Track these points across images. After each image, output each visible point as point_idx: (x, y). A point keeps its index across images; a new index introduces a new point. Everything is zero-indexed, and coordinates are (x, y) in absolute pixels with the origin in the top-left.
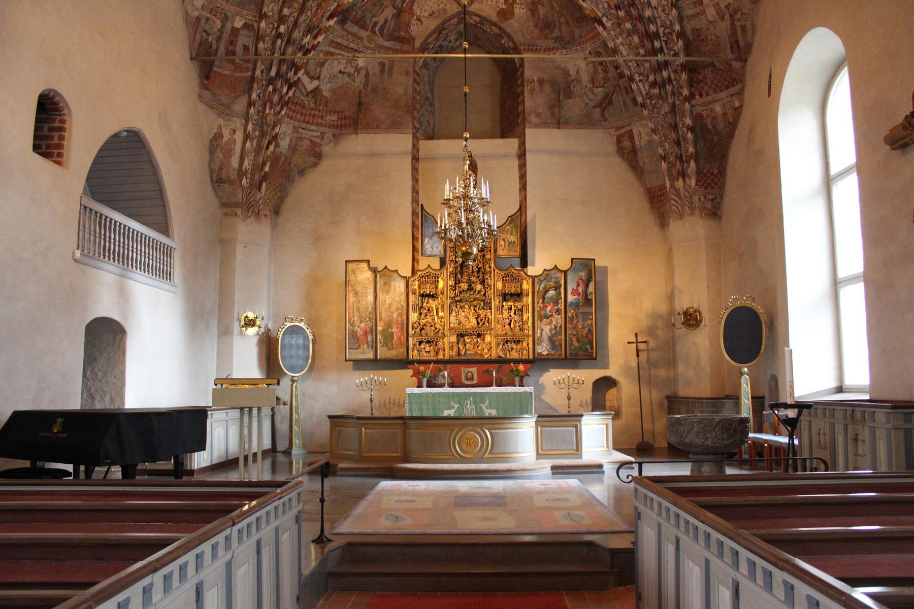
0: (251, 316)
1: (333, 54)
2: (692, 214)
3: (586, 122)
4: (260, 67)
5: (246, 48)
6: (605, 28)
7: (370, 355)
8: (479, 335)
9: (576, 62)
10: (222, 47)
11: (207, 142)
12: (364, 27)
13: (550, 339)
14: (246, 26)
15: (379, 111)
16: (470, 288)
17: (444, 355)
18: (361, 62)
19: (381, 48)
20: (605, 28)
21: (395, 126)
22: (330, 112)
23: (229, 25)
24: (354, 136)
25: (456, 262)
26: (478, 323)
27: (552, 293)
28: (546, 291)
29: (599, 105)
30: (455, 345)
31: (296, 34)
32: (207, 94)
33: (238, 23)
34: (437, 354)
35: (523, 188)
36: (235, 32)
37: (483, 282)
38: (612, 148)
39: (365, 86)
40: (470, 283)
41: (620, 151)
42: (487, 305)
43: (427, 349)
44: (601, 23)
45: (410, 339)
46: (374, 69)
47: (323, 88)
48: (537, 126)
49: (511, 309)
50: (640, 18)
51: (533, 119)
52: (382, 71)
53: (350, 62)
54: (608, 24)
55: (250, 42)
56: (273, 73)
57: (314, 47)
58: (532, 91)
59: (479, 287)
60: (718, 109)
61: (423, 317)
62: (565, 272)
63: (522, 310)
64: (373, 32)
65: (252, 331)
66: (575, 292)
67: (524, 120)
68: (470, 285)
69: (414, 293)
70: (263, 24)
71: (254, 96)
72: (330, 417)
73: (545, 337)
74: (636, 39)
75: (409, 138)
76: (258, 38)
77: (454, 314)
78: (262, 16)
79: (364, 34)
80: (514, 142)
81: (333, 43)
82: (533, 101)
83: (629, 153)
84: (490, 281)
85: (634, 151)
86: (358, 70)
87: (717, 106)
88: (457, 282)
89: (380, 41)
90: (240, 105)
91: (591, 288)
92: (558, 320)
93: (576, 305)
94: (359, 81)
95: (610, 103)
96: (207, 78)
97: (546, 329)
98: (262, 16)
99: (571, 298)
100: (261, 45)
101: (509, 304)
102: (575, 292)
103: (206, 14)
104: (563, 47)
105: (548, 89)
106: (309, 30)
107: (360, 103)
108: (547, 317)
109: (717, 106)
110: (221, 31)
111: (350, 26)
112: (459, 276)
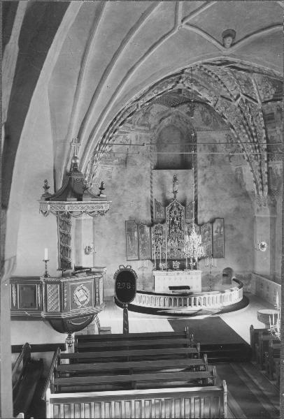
7: (137, 258)
12: (131, 123)
16: (175, 230)
19: (137, 130)
27: (207, 232)
28: (205, 231)
31: (107, 134)
40: (175, 228)
46: (133, 139)
52: (137, 139)
66: (216, 232)
89: (137, 127)
99: (215, 234)
102: (216, 232)
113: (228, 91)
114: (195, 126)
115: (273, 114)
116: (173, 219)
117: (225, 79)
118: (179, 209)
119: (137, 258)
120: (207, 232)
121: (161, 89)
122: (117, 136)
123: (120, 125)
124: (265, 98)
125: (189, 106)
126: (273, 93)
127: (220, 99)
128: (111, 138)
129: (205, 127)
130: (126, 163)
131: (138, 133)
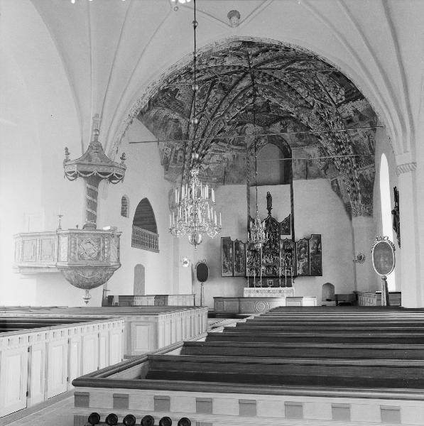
0: (186, 260)
1: (214, 154)
2: (360, 215)
3: (318, 175)
4: (186, 162)
5: (181, 157)
6: (321, 139)
9: (313, 151)
10: (172, 158)
11: (168, 195)
13: (303, 268)
14: (180, 149)
15: (233, 175)
16: (270, 247)
18: (225, 156)
20: (321, 139)
21: (240, 182)
22: (213, 177)
23: (174, 150)
24: (222, 186)
27: (303, 249)
28: (301, 248)
29: (323, 168)
31: (199, 150)
32: (167, 176)
33: (178, 148)
35: (292, 205)
36: (177, 152)
37: (276, 245)
38: (329, 187)
39: (227, 165)
41: (333, 187)
42: (278, 255)
44: (320, 138)
46: (231, 158)
47: (210, 167)
48: (298, 179)
50: (334, 137)
51: (296, 176)
53: (221, 156)
54: (323, 138)
55: (182, 155)
56: (191, 166)
57: (206, 154)
58: (295, 164)
60: (367, 171)
62: (308, 240)
64: (229, 143)
65: (186, 265)
67: (292, 178)
70: (187, 148)
71: (185, 174)
72: (214, 298)
73: (301, 267)
74: (334, 144)
75: (245, 186)
76: (185, 154)
78: (186, 145)
79: (225, 145)
80: (289, 185)
81: (214, 150)
82: (296, 168)
83: (337, 190)
85: (338, 187)
86: (224, 159)
87: (367, 171)
89: (232, 146)
90: (179, 178)
91: (319, 247)
92: (306, 260)
93: (312, 254)
94: (224, 164)
95: (328, 168)
96: (167, 170)
97: (300, 264)
98: (186, 145)
99: (311, 251)
100: (186, 156)
103: (166, 147)
104: (308, 145)
105: (302, 163)
106: (204, 148)
107: (225, 173)
108: (301, 259)
109: (367, 171)
110: (171, 152)
111: (220, 143)
113: (302, 98)
114: (289, 142)
115: (350, 116)
117: (295, 85)
118: (273, 225)
119: (231, 275)
120: (303, 249)
121: (243, 105)
122: (212, 155)
123: (212, 142)
124: (337, 100)
125: (281, 124)
126: (343, 93)
127: (299, 108)
128: (204, 156)
129: (299, 143)
130: (224, 181)
131: (234, 153)
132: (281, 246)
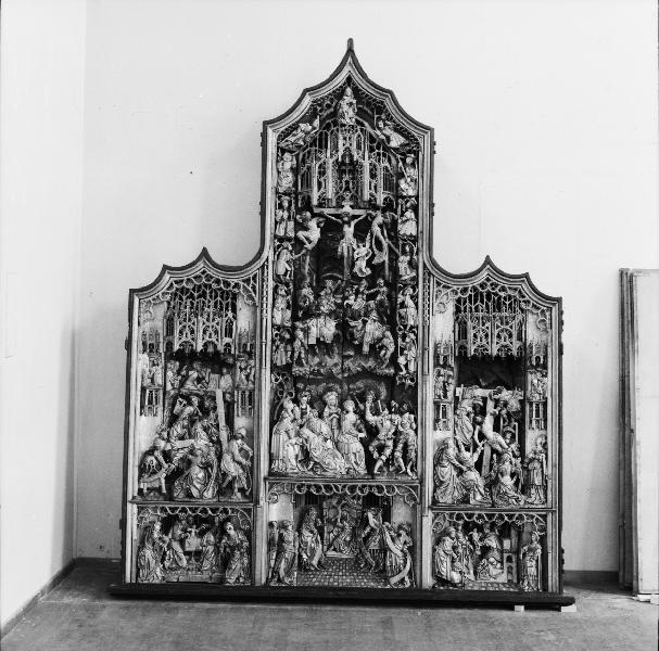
8: (371, 501)
17: (250, 570)
25: (298, 244)
26: (370, 462)
30: (290, 535)
34: (225, 563)
37: (390, 316)
40: (343, 316)
42: (403, 396)
43: (193, 543)
45: (132, 509)
49: (482, 411)
59: (373, 329)
61: (178, 429)
63: (519, 418)
68: (343, 327)
69: (150, 348)
77: (287, 423)
84: (411, 315)
88: (302, 312)
101: (480, 392)
112: (306, 291)
116: (332, 229)
118: (379, 146)
132: (442, 327)
